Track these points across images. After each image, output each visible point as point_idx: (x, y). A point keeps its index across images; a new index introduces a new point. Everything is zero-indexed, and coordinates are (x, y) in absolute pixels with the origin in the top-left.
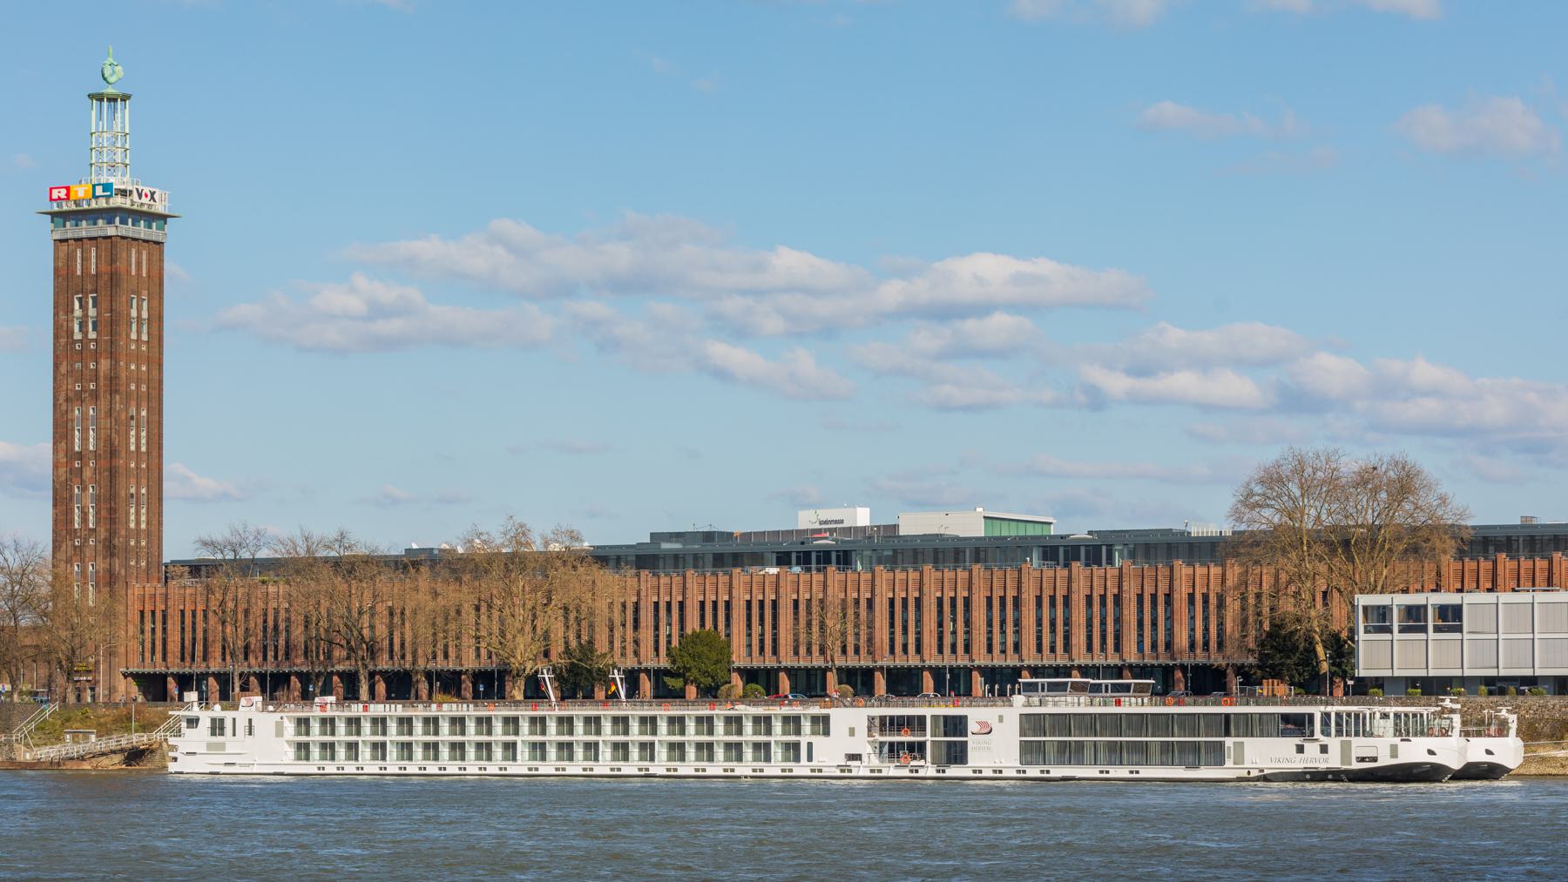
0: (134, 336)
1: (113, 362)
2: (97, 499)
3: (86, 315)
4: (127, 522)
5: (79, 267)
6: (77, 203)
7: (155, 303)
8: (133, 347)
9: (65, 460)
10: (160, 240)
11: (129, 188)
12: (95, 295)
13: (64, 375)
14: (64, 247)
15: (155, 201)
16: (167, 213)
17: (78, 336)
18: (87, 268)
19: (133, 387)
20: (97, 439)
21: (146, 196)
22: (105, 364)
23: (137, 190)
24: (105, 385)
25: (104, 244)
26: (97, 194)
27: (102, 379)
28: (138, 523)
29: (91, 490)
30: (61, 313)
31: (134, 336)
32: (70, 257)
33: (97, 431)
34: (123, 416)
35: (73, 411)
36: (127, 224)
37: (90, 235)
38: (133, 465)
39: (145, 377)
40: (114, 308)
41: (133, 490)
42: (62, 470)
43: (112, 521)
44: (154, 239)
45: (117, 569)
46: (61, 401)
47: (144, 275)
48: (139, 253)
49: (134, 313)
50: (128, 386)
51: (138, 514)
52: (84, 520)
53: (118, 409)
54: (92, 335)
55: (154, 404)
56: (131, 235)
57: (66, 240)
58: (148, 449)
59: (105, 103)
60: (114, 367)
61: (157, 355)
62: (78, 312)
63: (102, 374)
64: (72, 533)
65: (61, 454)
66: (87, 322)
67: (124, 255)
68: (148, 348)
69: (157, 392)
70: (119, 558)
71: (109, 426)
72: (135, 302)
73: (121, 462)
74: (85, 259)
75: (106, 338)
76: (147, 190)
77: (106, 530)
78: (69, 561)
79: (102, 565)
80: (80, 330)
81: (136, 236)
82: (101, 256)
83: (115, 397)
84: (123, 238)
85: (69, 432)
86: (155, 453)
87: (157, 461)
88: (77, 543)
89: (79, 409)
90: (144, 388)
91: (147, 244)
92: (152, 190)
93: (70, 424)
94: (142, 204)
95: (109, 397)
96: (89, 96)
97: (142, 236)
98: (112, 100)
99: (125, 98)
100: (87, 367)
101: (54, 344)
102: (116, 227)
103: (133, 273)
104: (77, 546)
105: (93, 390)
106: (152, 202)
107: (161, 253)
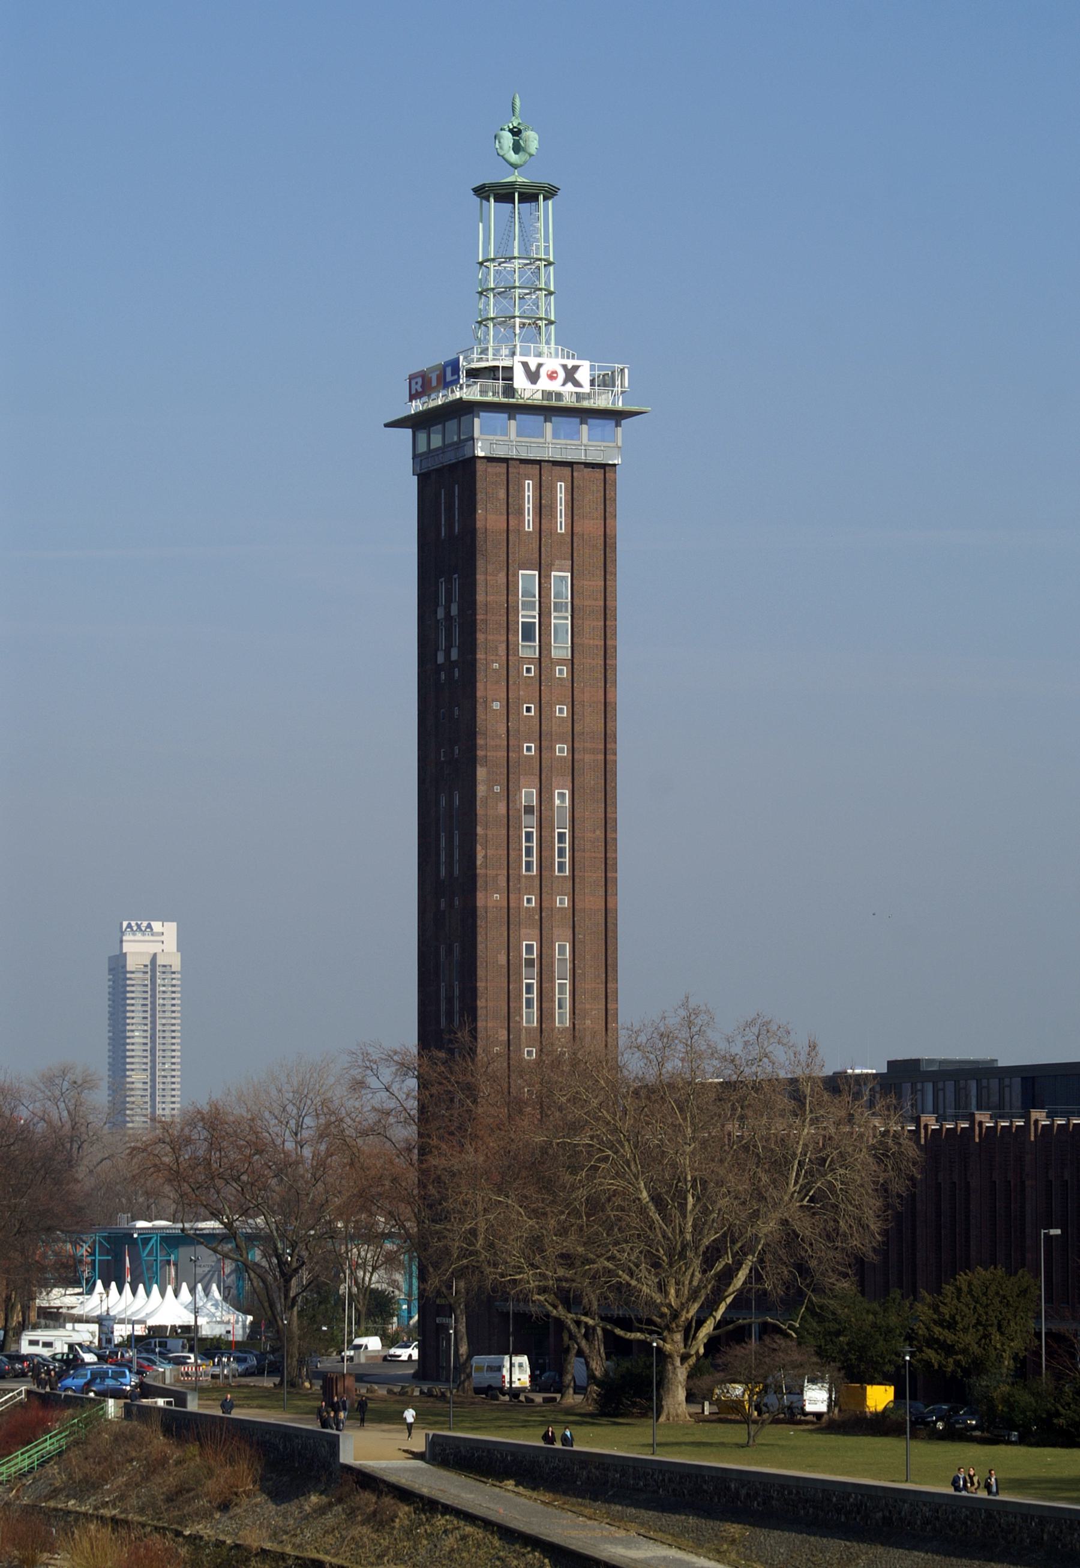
15: (577, 384)
16: (620, 405)
19: (529, 749)
23: (525, 365)
55: (591, 779)
56: (514, 454)
91: (567, 471)
92: (570, 363)
97: (549, 454)
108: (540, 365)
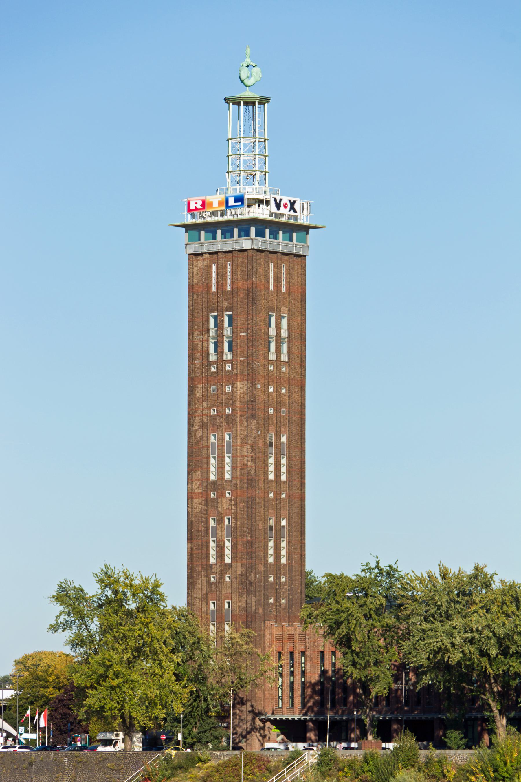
0: (272, 357)
1: (249, 385)
2: (234, 533)
3: (221, 335)
4: (266, 555)
5: (214, 282)
6: (214, 214)
7: (297, 320)
8: (271, 368)
9: (200, 490)
10: (301, 253)
11: (266, 197)
12: (231, 313)
13: (198, 399)
14: (199, 263)
15: (295, 211)
16: (308, 223)
17: (213, 357)
18: (222, 284)
20: (233, 467)
21: (285, 207)
22: (241, 387)
23: (275, 199)
24: (241, 410)
25: (240, 258)
26: (230, 204)
27: (237, 403)
28: (277, 557)
29: (227, 521)
30: (196, 333)
31: (272, 357)
32: (207, 271)
33: (234, 458)
34: (261, 443)
35: (208, 438)
36: (263, 236)
37: (224, 249)
38: (271, 495)
39: (285, 400)
40: (250, 326)
41: (272, 522)
42: (198, 501)
43: (250, 555)
44: (294, 251)
45: (254, 607)
46: (196, 427)
47: (284, 290)
48: (278, 268)
49: (272, 332)
50: (266, 410)
51: (277, 548)
52: (220, 554)
53: (254, 435)
54: (228, 356)
55: (296, 429)
56: (268, 248)
57: (201, 254)
58: (288, 477)
59: (242, 107)
60: (252, 390)
61: (299, 376)
62: (213, 332)
63: (237, 398)
64: (208, 568)
65: (196, 484)
66: (223, 342)
67: (262, 270)
68: (289, 369)
69: (299, 416)
70: (255, 596)
71: (245, 454)
72: (273, 319)
73: (258, 491)
74: (221, 274)
75: (243, 359)
76: (286, 200)
77: (243, 566)
78: (205, 599)
79: (239, 603)
80: (216, 351)
81: (274, 249)
82: (236, 272)
83: (251, 423)
84: (258, 251)
85: (205, 461)
86: (297, 483)
87: (298, 491)
88: (212, 580)
89: (214, 436)
90: (284, 412)
92: (292, 199)
93: (205, 452)
94: (281, 215)
95: (244, 422)
96: (225, 99)
97: (281, 249)
98: (250, 103)
99: (264, 101)
100: (223, 390)
101: (189, 366)
102: (252, 239)
103: (271, 288)
104: (213, 583)
105: (228, 415)
106: (292, 213)
107: (304, 267)
108: (281, 200)
